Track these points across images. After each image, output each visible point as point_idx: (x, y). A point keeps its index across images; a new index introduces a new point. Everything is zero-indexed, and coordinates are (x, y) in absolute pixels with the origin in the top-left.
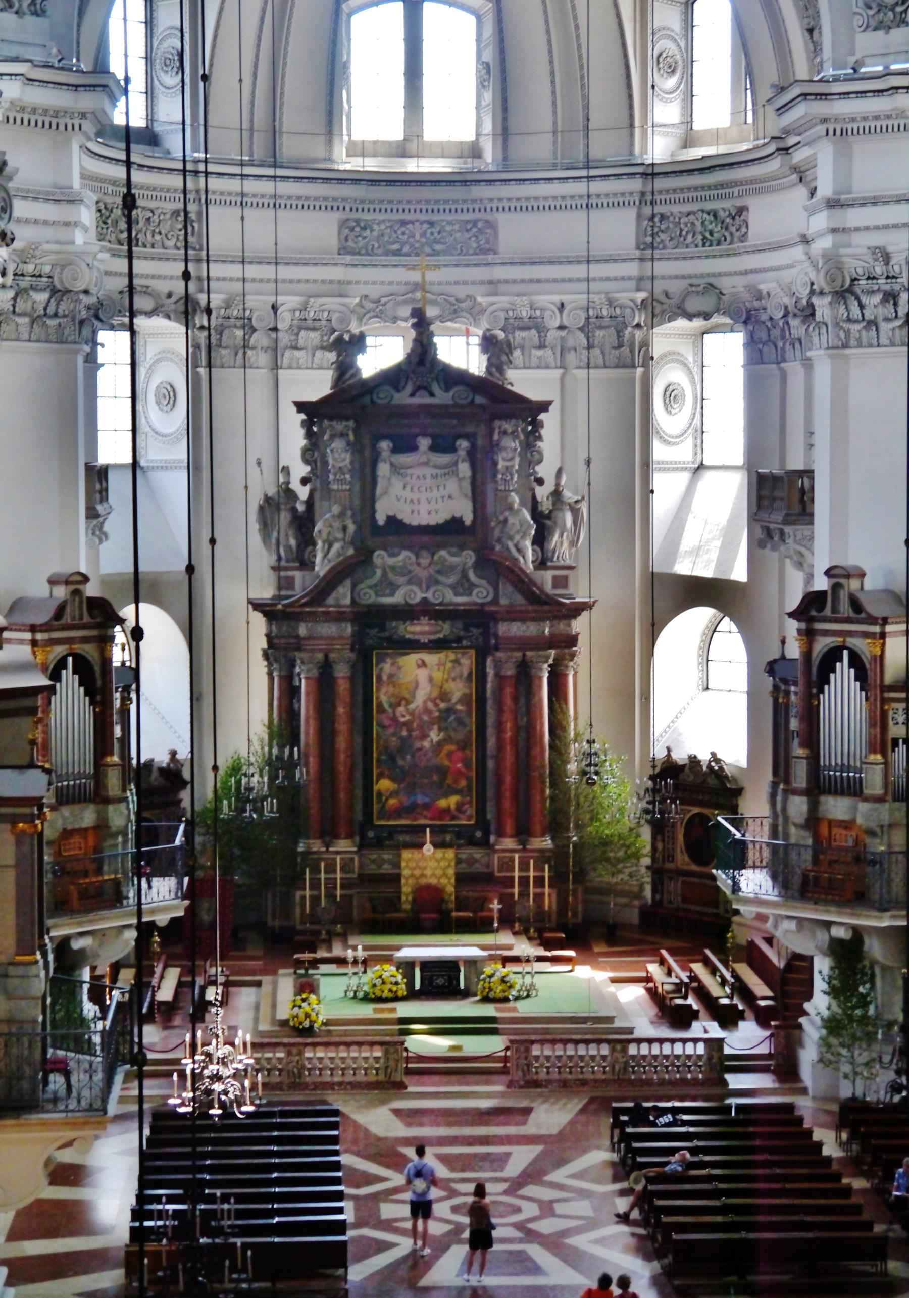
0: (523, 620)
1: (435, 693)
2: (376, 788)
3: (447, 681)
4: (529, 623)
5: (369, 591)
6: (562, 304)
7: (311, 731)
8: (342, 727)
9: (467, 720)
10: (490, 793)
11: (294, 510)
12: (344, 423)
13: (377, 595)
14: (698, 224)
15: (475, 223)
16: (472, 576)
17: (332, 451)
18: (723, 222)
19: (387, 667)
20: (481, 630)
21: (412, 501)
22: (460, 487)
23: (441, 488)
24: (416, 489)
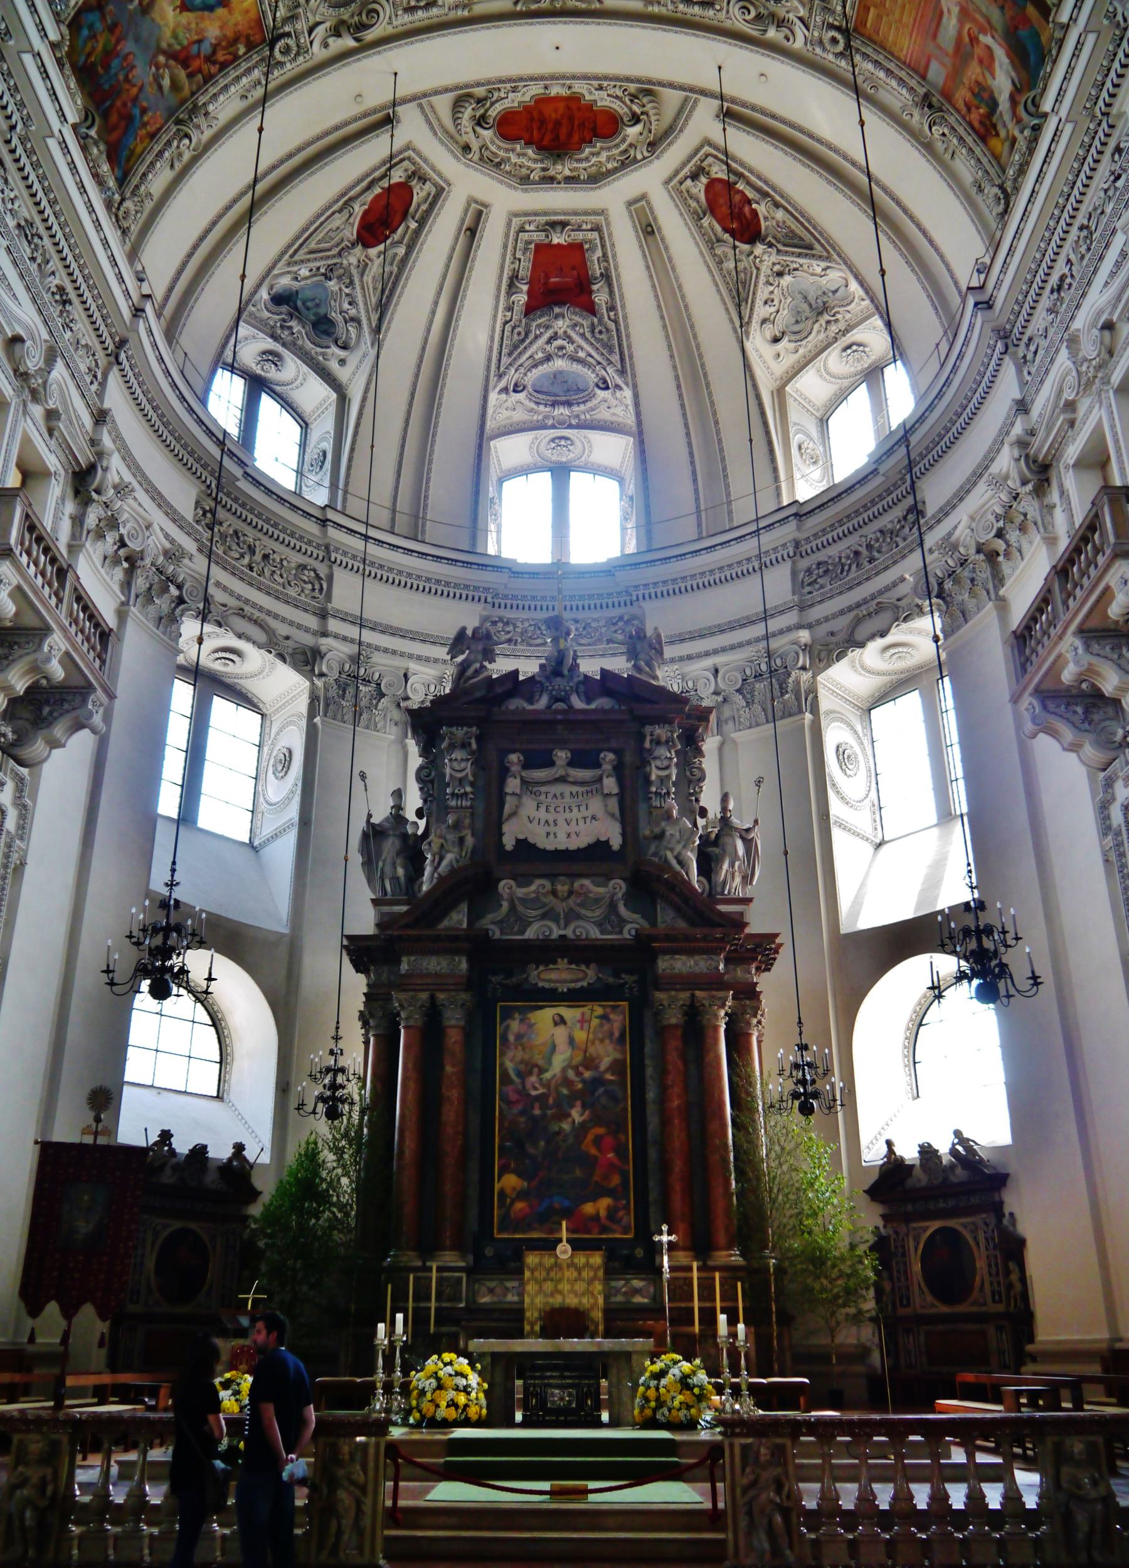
0: (691, 952)
1: (579, 1059)
2: (497, 1187)
3: (593, 1043)
4: (697, 958)
5: (492, 927)
6: (717, 671)
7: (410, 1097)
8: (453, 1094)
9: (620, 1095)
10: (653, 1196)
11: (405, 836)
12: (465, 729)
13: (502, 933)
14: (863, 550)
15: (621, 618)
16: (622, 909)
17: (450, 760)
18: (892, 533)
19: (515, 1025)
20: (635, 978)
21: (547, 822)
22: (606, 806)
23: (583, 808)
24: (552, 809)
